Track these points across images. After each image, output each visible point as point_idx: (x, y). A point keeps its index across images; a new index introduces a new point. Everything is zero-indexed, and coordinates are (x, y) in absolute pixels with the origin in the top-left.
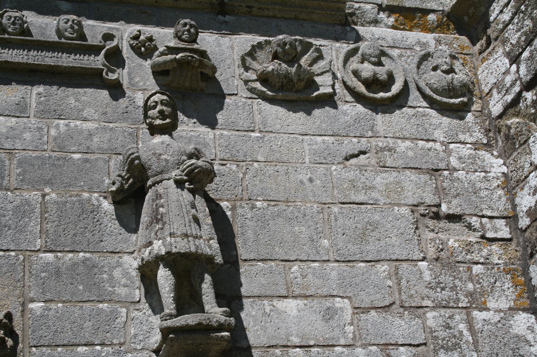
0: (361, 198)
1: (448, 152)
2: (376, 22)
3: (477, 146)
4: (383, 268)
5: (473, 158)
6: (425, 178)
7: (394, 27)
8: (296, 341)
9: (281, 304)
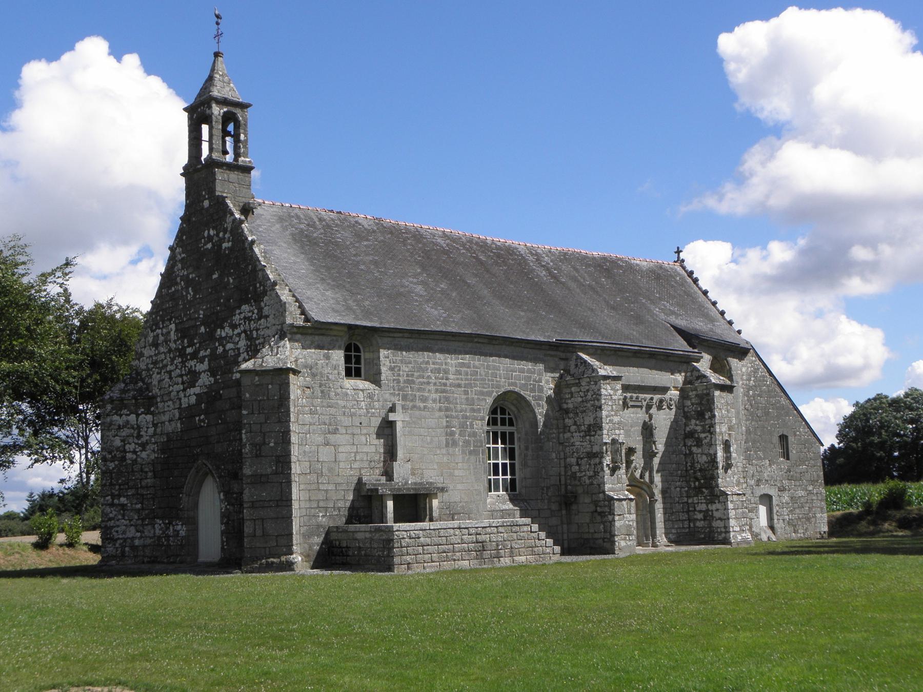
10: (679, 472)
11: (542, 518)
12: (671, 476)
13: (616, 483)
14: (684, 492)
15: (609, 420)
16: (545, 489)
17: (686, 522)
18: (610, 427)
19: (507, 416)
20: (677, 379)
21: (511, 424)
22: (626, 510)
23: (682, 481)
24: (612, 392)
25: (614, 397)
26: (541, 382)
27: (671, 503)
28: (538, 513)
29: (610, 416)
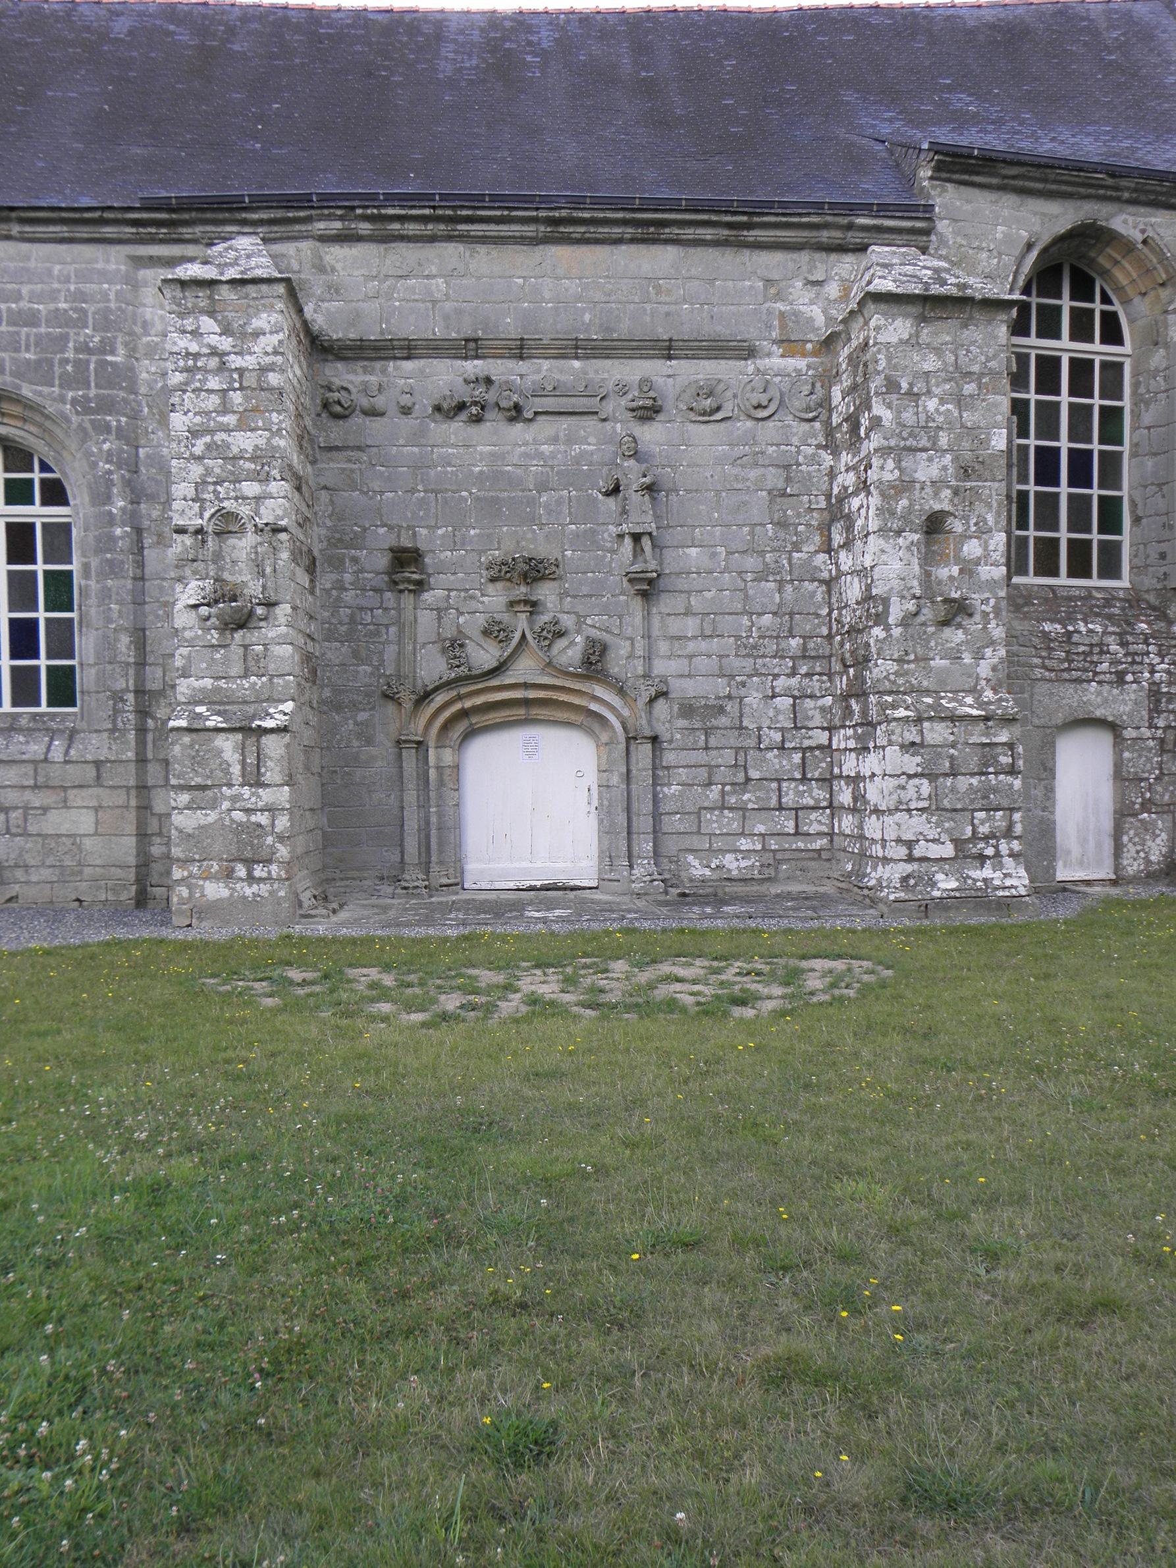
0: (740, 486)
1: (798, 452)
2: (769, 355)
3: (819, 447)
4: (746, 529)
5: (814, 455)
6: (780, 471)
7: (782, 356)
8: (694, 570)
9: (687, 550)
10: (794, 643)
11: (111, 787)
12: (748, 656)
13: (236, 669)
14: (817, 715)
15: (208, 447)
16: (130, 697)
17: (814, 815)
18: (208, 471)
19: (36, 476)
20: (796, 314)
21: (55, 493)
22: (236, 770)
23: (809, 675)
24: (225, 343)
25: (235, 361)
26: (113, 352)
27: (737, 750)
28: (94, 773)
29: (212, 432)
